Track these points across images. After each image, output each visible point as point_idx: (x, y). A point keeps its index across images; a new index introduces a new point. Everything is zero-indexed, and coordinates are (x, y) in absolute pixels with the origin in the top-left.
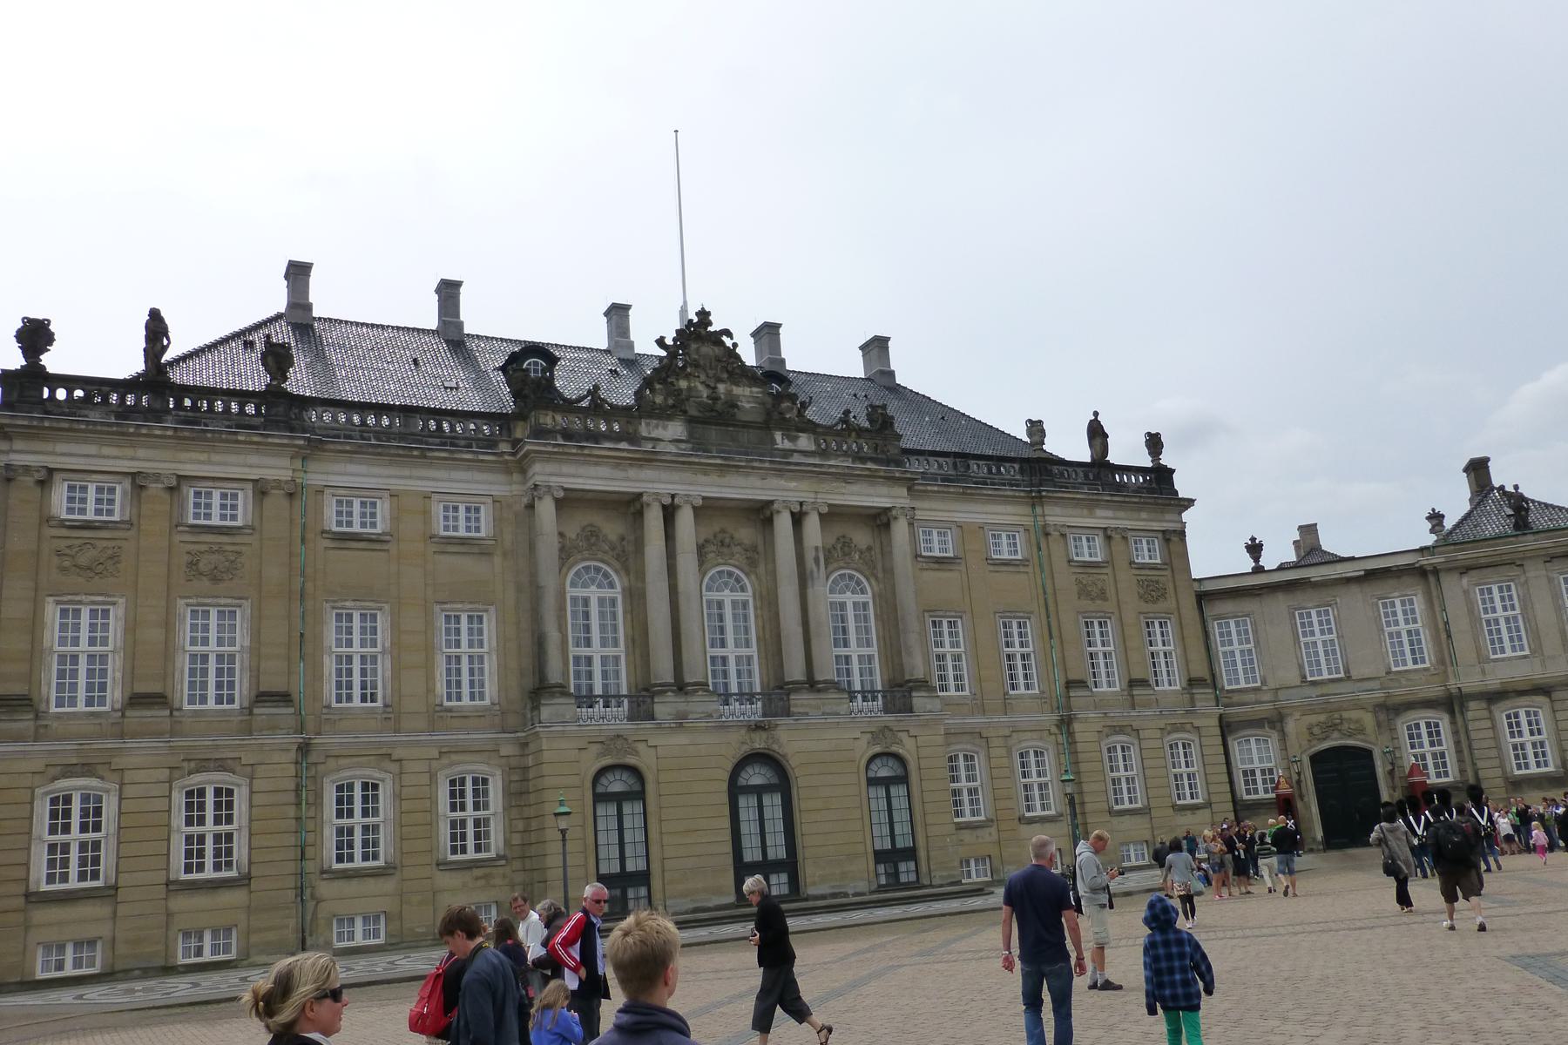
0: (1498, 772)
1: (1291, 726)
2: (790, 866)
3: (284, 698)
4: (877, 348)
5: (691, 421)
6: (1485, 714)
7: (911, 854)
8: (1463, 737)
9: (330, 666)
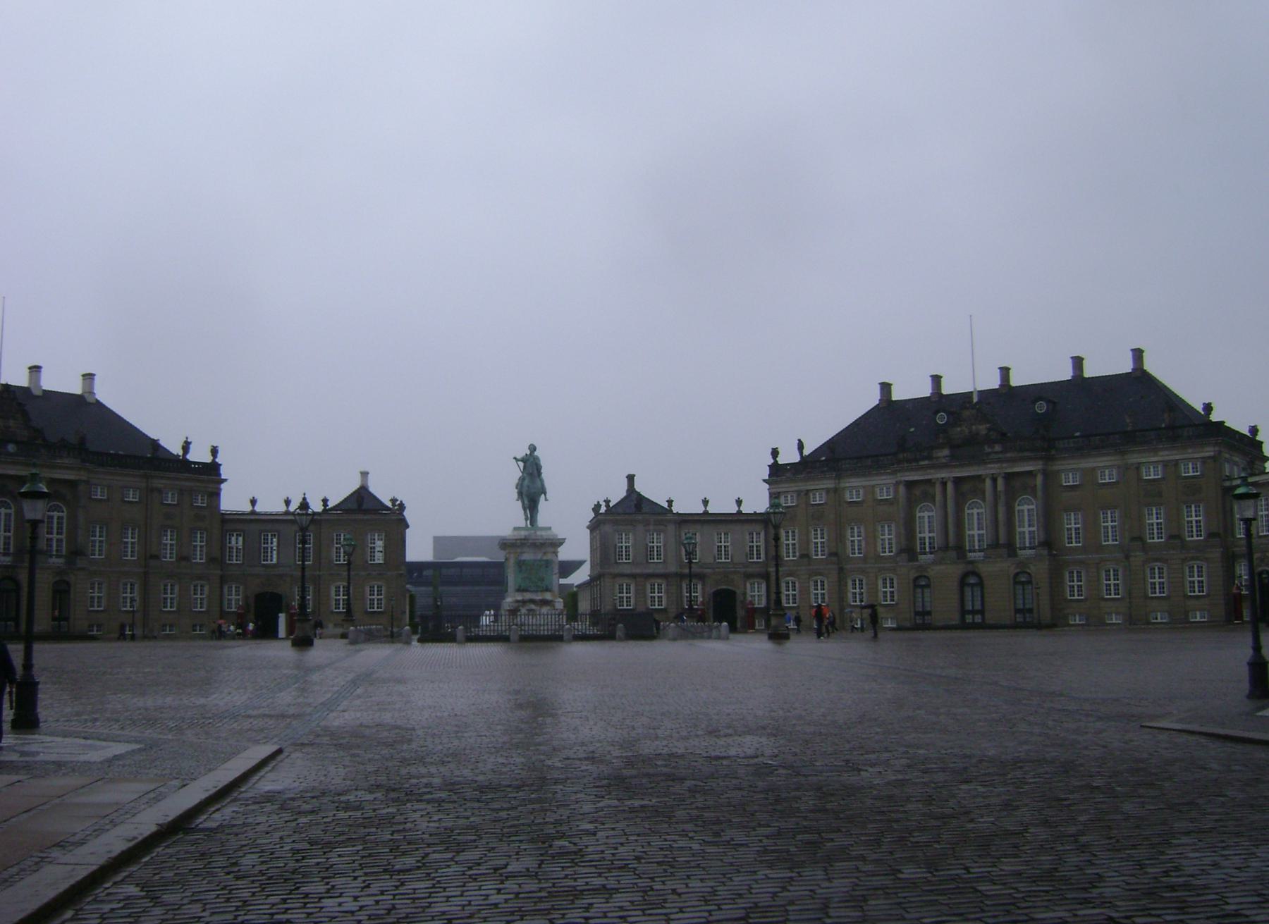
2: (982, 612)
3: (836, 554)
4: (1138, 354)
5: (953, 447)
7: (1030, 611)
9: (849, 544)
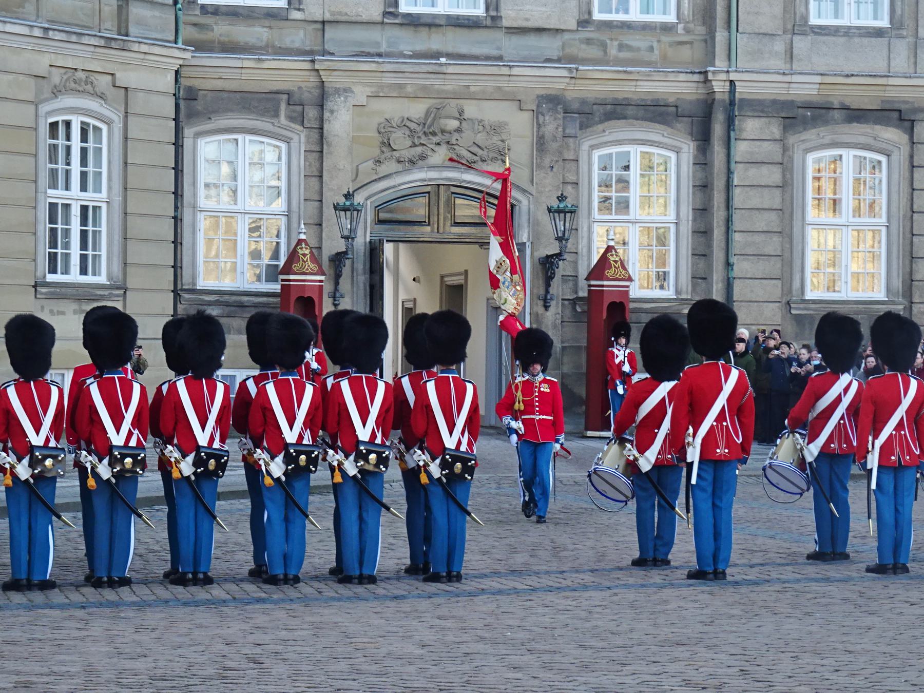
0: (774, 289)
1: (341, 121)
6: (772, 150)
8: (718, 198)
